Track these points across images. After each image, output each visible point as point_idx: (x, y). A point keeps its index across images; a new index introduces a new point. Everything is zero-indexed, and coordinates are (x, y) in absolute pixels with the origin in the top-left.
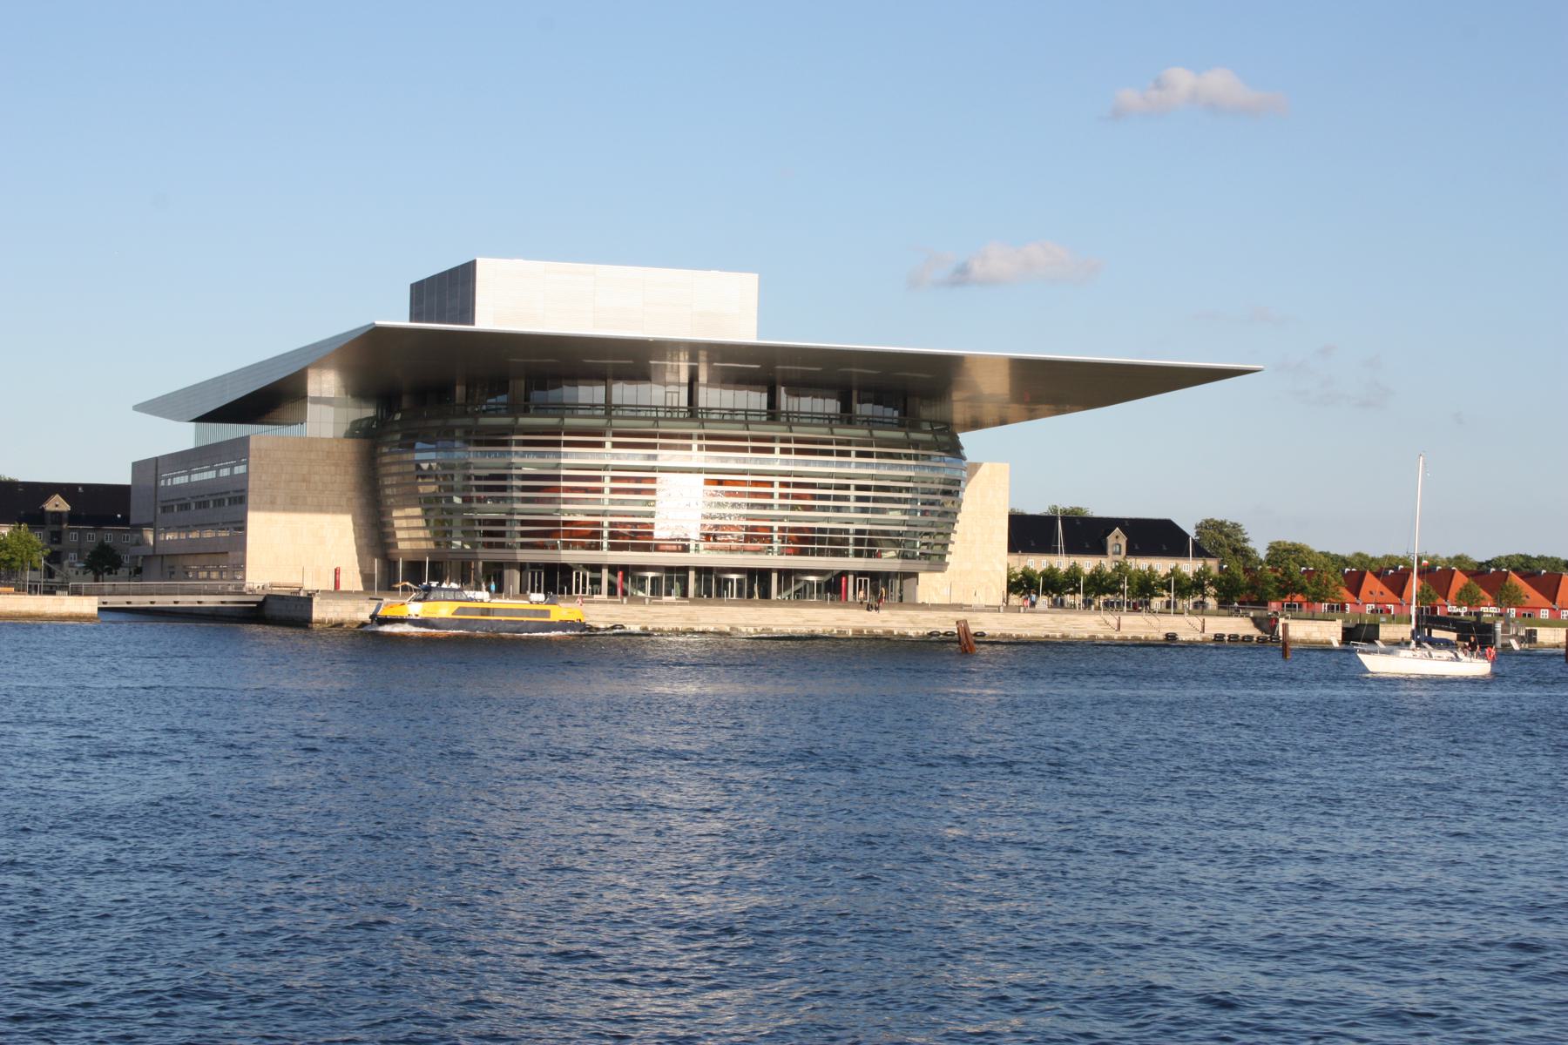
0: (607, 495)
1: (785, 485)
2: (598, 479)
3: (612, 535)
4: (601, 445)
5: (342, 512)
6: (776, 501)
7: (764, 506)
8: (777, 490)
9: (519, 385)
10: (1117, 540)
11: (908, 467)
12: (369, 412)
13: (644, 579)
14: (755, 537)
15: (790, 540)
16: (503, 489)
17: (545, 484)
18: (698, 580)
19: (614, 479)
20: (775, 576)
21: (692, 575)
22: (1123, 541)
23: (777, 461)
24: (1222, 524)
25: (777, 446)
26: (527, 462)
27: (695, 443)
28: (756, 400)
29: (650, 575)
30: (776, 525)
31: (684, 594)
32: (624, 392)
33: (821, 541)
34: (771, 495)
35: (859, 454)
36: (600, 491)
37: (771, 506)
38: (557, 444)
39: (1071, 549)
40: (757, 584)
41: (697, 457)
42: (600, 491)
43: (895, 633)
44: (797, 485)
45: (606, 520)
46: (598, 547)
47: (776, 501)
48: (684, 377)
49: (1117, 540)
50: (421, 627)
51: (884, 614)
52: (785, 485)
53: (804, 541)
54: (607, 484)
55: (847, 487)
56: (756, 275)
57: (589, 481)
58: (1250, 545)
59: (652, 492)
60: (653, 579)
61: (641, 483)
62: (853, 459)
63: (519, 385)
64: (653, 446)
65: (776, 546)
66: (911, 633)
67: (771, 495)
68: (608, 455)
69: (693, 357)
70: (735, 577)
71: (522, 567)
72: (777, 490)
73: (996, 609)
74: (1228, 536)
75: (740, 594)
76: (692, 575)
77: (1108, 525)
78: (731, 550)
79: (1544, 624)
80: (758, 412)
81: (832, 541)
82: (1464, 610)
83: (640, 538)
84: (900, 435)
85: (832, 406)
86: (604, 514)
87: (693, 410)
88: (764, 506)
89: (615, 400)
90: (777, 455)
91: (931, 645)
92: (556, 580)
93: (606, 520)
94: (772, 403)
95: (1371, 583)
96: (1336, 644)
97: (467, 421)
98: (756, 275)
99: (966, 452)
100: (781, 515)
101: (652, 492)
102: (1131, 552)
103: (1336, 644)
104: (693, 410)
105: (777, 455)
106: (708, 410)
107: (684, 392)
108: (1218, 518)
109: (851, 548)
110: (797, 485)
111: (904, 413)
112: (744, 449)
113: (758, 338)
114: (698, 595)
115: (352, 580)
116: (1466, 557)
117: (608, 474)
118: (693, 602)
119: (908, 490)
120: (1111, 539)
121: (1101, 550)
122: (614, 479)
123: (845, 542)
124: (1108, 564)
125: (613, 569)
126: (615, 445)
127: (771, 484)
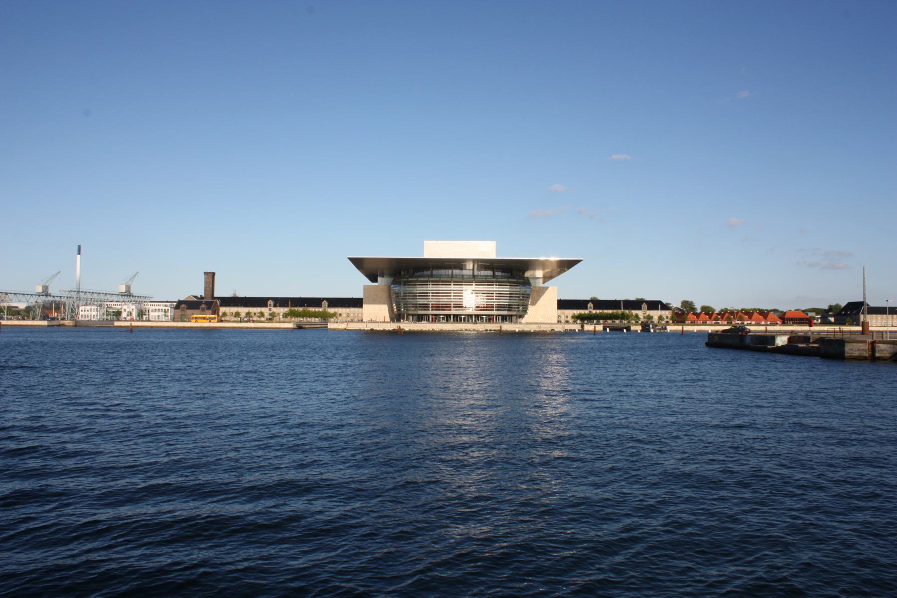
0: (452, 297)
1: (432, 293)
2: (451, 293)
3: (432, 307)
4: (451, 285)
5: (384, 304)
6: (495, 298)
7: (491, 299)
8: (495, 295)
9: (411, 271)
10: (325, 303)
11: (507, 288)
12: (392, 279)
13: (483, 318)
14: (489, 307)
15: (498, 307)
16: (427, 296)
17: (425, 295)
18: (454, 318)
19: (454, 293)
20: (452, 316)
21: (474, 316)
22: (646, 306)
23: (495, 288)
24: (688, 302)
25: (452, 284)
26: (419, 289)
27: (474, 284)
28: (490, 273)
29: (463, 317)
30: (495, 304)
31: (429, 321)
32: (457, 272)
33: (442, 307)
34: (493, 296)
35: (432, 285)
36: (451, 296)
37: (493, 299)
38: (416, 285)
39: (625, 308)
40: (490, 319)
41: (474, 287)
42: (451, 296)
43: (695, 331)
44: (500, 295)
45: (431, 303)
46: (428, 310)
47: (431, 297)
48: (472, 268)
49: (325, 303)
50: (334, 329)
51: (478, 325)
52: (432, 293)
53: (500, 308)
54: (452, 294)
55: (493, 294)
56: (425, 241)
57: (425, 295)
58: (695, 307)
59: (462, 296)
60: (464, 318)
61: (459, 294)
62: (431, 286)
63: (411, 271)
64: (462, 285)
65: (495, 309)
66: (391, 329)
67: (493, 296)
68: (452, 287)
69: (474, 263)
70: (484, 317)
71: (413, 315)
72: (431, 294)
73: (555, 324)
74: (690, 304)
75: (464, 321)
76: (474, 316)
77: (268, 299)
78: (481, 310)
79: (633, 325)
80: (491, 276)
81: (442, 307)
82: (740, 322)
83: (459, 306)
84: (506, 280)
85: (509, 275)
86: (451, 302)
87: (474, 275)
88: (491, 299)
89: (454, 274)
90: (452, 286)
91: (523, 334)
92: (420, 318)
93: (431, 303)
94: (494, 273)
95: (756, 315)
96: (639, 332)
97: (406, 279)
98: (425, 241)
99: (532, 284)
100: (495, 302)
101: (462, 296)
102: (329, 306)
103: (639, 332)
104: (474, 275)
105: (452, 286)
106: (456, 275)
107: (472, 271)
108: (687, 300)
109: (495, 309)
110: (436, 293)
111: (511, 275)
112: (485, 285)
113: (496, 256)
114: (432, 321)
115: (388, 319)
116: (712, 308)
117: (452, 292)
118: (430, 323)
119: (517, 294)
120: (589, 305)
121: (586, 308)
122: (454, 293)
123: (454, 307)
124: (586, 312)
125: (432, 315)
126: (454, 285)
127: (493, 294)
